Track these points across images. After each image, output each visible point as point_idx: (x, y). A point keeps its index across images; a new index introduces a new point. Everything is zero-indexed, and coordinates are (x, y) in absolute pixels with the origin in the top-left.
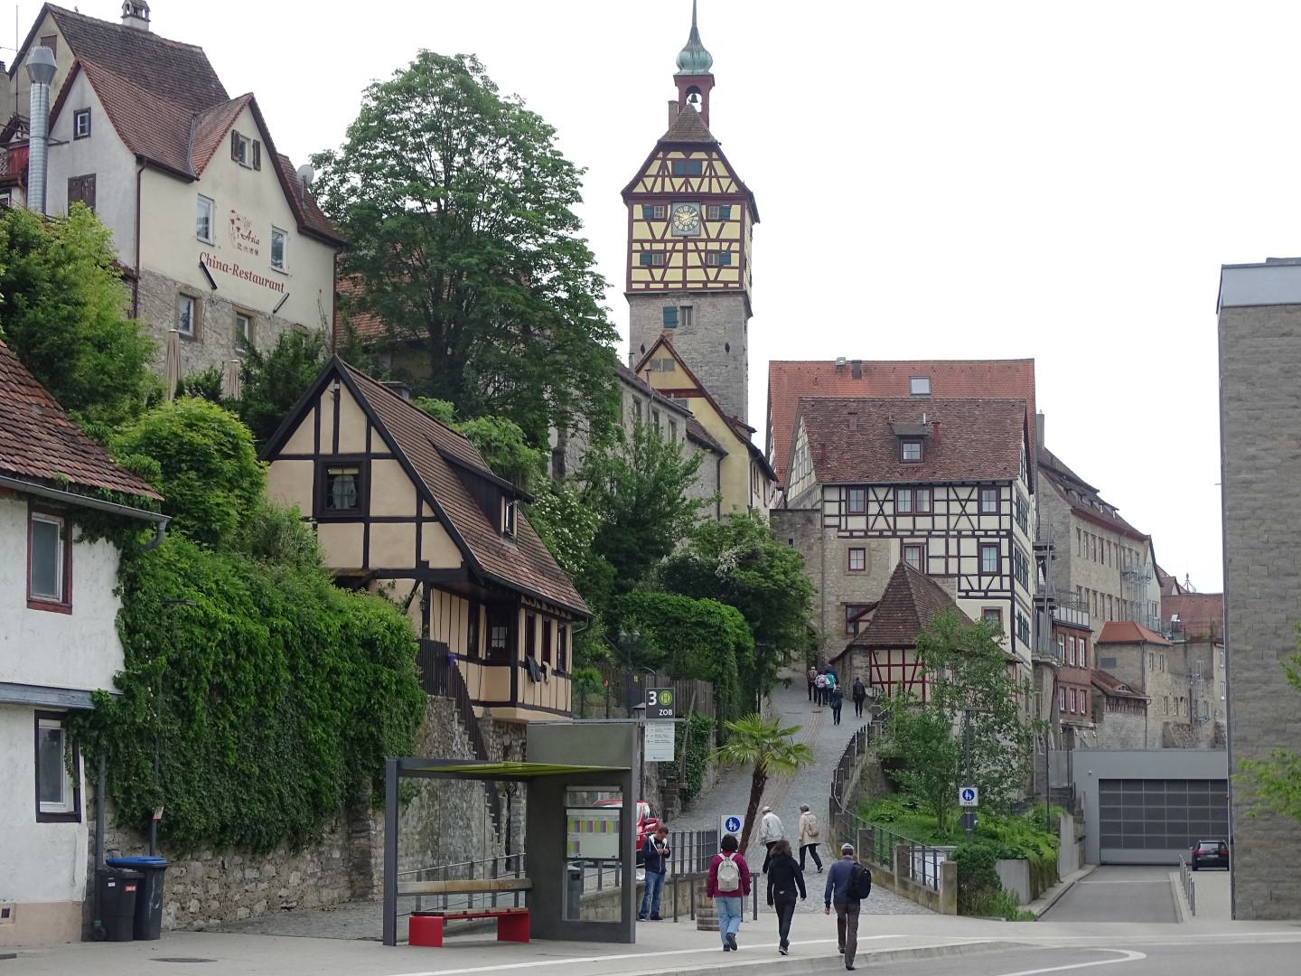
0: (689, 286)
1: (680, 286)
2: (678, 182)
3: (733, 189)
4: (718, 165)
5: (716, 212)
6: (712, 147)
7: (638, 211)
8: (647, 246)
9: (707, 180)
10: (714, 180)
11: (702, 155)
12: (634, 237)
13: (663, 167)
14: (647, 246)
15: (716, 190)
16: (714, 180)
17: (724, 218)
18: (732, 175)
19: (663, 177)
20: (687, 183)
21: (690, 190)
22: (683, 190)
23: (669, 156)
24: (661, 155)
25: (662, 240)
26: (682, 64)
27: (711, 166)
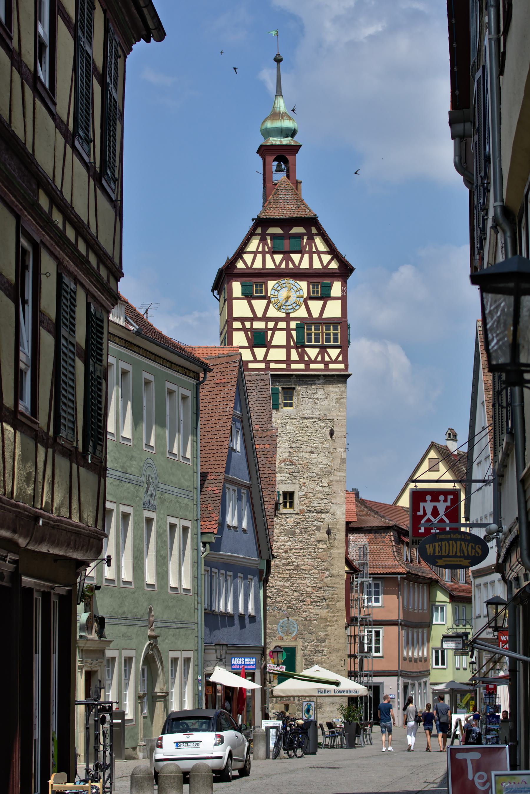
0: (293, 366)
1: (284, 366)
2: (278, 258)
3: (334, 265)
4: (318, 241)
7: (237, 288)
8: (248, 325)
9: (306, 256)
10: (315, 256)
11: (300, 230)
12: (235, 315)
14: (248, 325)
15: (317, 265)
16: (315, 256)
17: (325, 297)
19: (264, 253)
21: (291, 266)
22: (283, 266)
23: (267, 232)
24: (259, 231)
25: (265, 319)
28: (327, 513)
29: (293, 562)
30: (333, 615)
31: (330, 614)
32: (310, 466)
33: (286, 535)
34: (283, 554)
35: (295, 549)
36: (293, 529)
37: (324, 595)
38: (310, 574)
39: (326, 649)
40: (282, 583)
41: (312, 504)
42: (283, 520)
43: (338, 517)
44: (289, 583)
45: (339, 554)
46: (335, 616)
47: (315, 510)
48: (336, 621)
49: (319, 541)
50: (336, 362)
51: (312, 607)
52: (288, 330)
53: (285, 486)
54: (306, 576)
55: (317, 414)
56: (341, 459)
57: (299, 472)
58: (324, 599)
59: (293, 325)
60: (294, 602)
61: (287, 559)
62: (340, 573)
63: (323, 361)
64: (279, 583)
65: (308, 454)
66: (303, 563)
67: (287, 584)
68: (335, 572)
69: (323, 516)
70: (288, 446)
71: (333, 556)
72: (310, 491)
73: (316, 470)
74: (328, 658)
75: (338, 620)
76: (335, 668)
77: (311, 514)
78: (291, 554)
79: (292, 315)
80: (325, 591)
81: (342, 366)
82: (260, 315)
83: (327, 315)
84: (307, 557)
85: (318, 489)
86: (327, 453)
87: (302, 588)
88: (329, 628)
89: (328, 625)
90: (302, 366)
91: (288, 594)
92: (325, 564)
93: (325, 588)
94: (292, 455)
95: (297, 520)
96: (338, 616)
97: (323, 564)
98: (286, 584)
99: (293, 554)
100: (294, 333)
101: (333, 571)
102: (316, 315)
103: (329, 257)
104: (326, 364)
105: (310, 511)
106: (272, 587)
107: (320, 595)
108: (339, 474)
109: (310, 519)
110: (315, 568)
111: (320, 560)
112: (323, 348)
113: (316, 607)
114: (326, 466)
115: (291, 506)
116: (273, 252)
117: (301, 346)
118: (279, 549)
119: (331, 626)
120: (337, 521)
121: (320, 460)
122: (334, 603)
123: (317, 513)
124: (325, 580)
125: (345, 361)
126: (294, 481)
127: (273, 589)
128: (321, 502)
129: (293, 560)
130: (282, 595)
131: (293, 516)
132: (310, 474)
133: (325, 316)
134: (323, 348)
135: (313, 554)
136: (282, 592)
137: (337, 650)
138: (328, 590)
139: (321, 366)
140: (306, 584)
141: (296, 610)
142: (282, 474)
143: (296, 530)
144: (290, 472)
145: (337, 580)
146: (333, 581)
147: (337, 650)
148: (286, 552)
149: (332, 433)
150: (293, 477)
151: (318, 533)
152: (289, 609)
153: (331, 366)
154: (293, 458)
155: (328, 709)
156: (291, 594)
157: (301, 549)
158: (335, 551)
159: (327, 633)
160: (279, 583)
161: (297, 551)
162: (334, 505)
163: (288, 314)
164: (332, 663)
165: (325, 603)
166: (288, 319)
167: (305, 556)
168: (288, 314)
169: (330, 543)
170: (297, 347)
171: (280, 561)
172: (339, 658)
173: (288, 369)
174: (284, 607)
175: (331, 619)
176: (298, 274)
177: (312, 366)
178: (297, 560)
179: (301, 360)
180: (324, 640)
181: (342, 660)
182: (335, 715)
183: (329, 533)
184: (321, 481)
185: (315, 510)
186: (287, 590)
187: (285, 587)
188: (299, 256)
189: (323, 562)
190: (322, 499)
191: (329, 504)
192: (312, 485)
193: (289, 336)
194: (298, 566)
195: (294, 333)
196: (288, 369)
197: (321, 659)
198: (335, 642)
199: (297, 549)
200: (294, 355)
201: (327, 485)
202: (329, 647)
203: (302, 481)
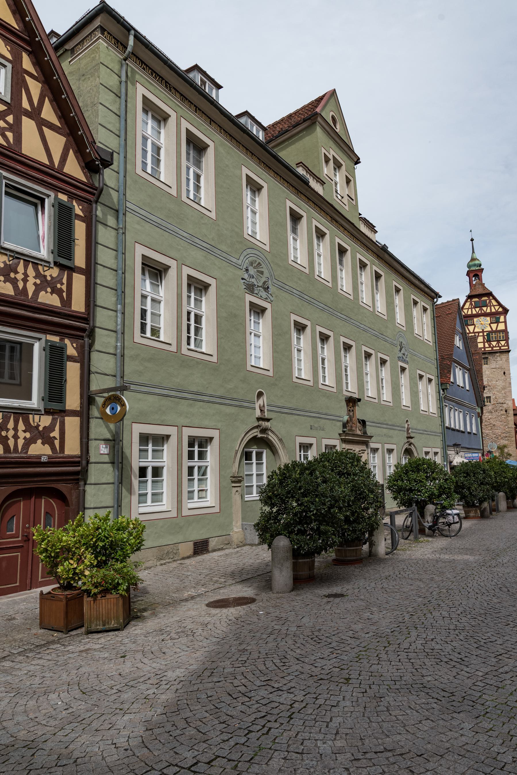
0: (487, 349)
2: (477, 309)
5: (494, 320)
6: (490, 294)
9: (489, 308)
10: (492, 307)
11: (486, 298)
13: (471, 304)
15: (493, 310)
16: (492, 307)
17: (498, 322)
18: (500, 304)
19: (471, 308)
20: (481, 309)
22: (480, 312)
24: (469, 300)
26: (469, 266)
27: (490, 302)
50: (504, 346)
52: (483, 336)
55: (498, 366)
59: (485, 334)
63: (499, 346)
67: (491, 432)
73: (499, 388)
79: (485, 330)
81: (507, 348)
82: (472, 331)
83: (498, 329)
90: (490, 349)
100: (486, 337)
102: (494, 329)
103: (498, 307)
104: (500, 347)
112: (498, 341)
115: (490, 402)
116: (475, 307)
117: (489, 341)
125: (508, 345)
133: (498, 329)
134: (498, 341)
139: (498, 348)
140: (498, 432)
145: (511, 429)
149: (504, 373)
153: (502, 348)
158: (509, 418)
163: (483, 330)
166: (483, 332)
168: (483, 330)
170: (487, 342)
173: (485, 350)
176: (486, 315)
177: (494, 349)
179: (490, 347)
183: (506, 411)
188: (486, 308)
193: (484, 338)
195: (486, 337)
196: (485, 350)
200: (487, 345)
203: (494, 392)
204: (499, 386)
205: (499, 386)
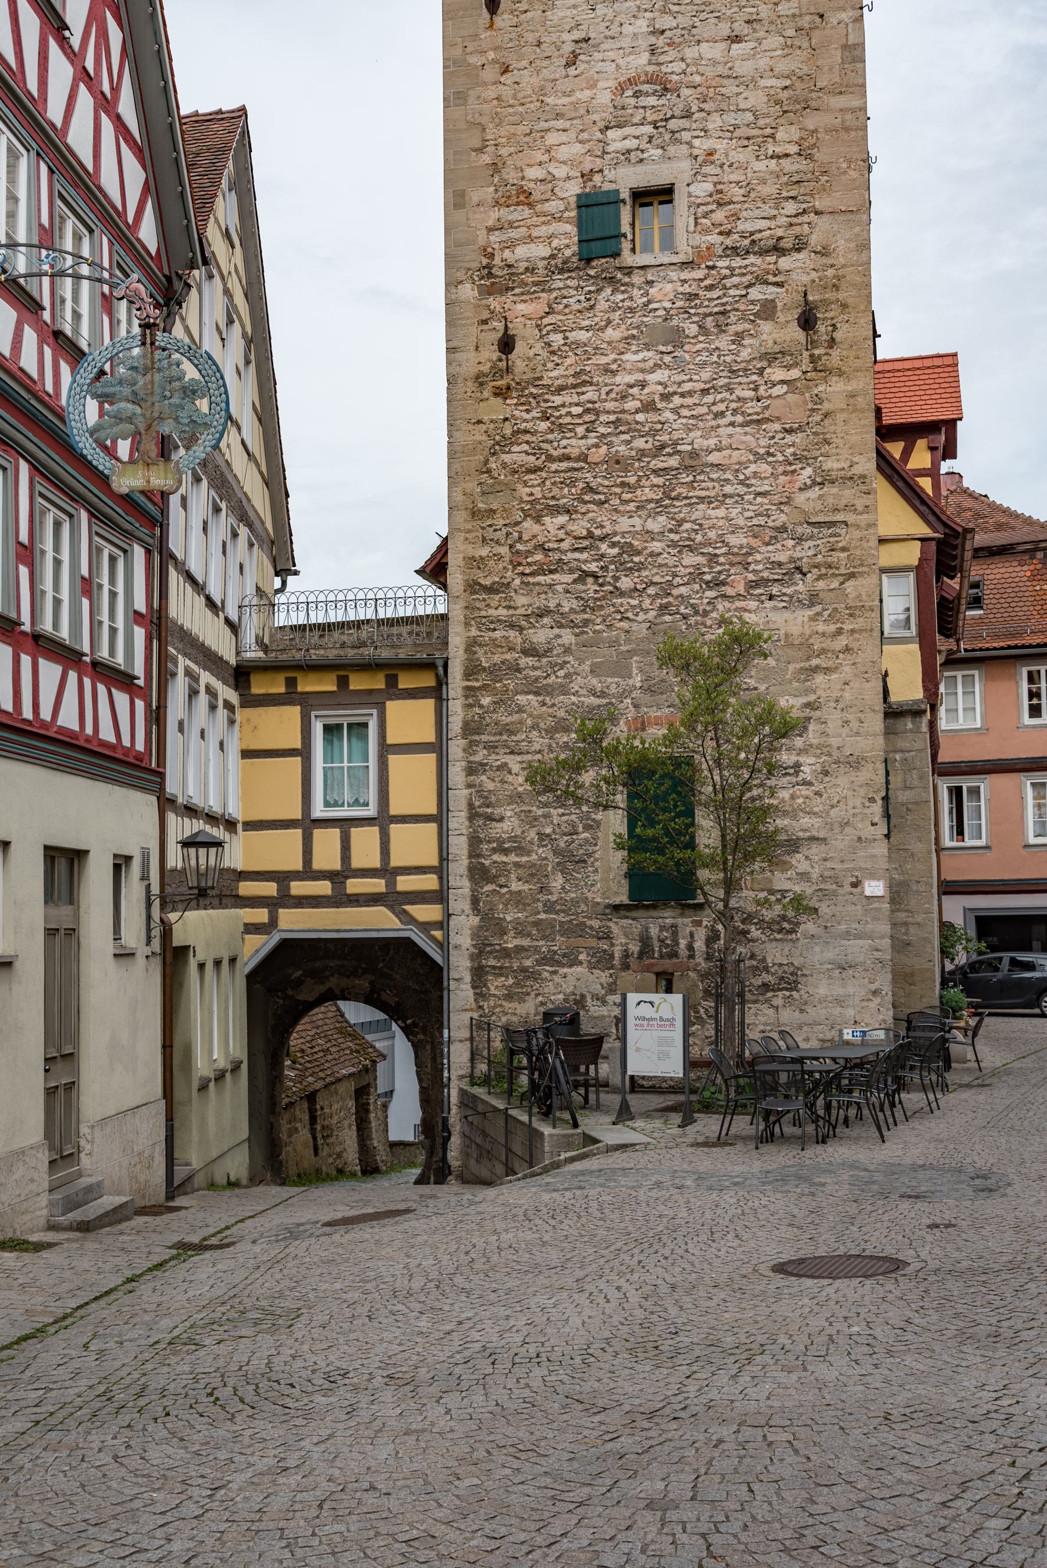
28: (799, 250)
29: (676, 443)
30: (832, 628)
31: (821, 627)
32: (730, 89)
33: (647, 347)
34: (640, 417)
35: (682, 395)
36: (675, 322)
37: (799, 555)
38: (741, 483)
39: (811, 760)
40: (637, 521)
41: (742, 226)
42: (636, 292)
43: (842, 260)
44: (662, 519)
45: (852, 396)
46: (839, 632)
47: (753, 242)
48: (847, 649)
49: (770, 358)
51: (753, 604)
53: (640, 168)
54: (728, 489)
56: (845, 47)
57: (687, 115)
58: (799, 569)
60: (683, 590)
61: (653, 433)
62: (857, 470)
64: (624, 523)
65: (723, 45)
66: (712, 442)
68: (836, 465)
69: (785, 263)
70: (645, 29)
71: (826, 406)
72: (734, 177)
73: (755, 99)
74: (818, 794)
75: (855, 645)
76: (848, 830)
77: (737, 262)
78: (668, 415)
80: (800, 539)
84: (729, 418)
85: (760, 166)
86: (791, 32)
87: (712, 534)
88: (820, 679)
89: (816, 669)
91: (660, 560)
92: (798, 438)
93: (799, 530)
94: (662, 59)
95: (686, 288)
96: (853, 631)
97: (789, 439)
98: (653, 525)
99: (675, 411)
101: (830, 464)
105: (734, 251)
106: (602, 539)
107: (782, 557)
108: (838, 102)
109: (736, 280)
110: (758, 457)
111: (777, 426)
113: (769, 604)
114: (788, 83)
115: (668, 244)
118: (624, 397)
119: (827, 670)
120: (834, 277)
121: (763, 63)
122: (835, 584)
123: (763, 252)
124: (800, 499)
126: (672, 150)
127: (604, 547)
128: (775, 212)
129: (676, 435)
130: (640, 567)
131: (673, 275)
132: (730, 119)
135: (752, 407)
136: (639, 553)
137: (855, 763)
138: (811, 537)
140: (726, 521)
141: (692, 620)
142: (628, 130)
143: (686, 325)
144: (655, 117)
146: (831, 501)
147: (855, 763)
148: (648, 407)
150: (667, 137)
151: (766, 326)
152: (668, 618)
154: (664, 68)
155: (822, 991)
156: (671, 562)
157: (705, 392)
158: (835, 389)
159: (812, 698)
160: (624, 523)
161: (689, 401)
162: (825, 218)
164: (834, 812)
165: (801, 587)
167: (721, 414)
169: (813, 360)
171: (628, 442)
172: (862, 792)
174: (646, 611)
175: (828, 643)
178: (692, 435)
180: (799, 727)
181: (872, 800)
182: (851, 1012)
183: (807, 321)
184: (772, 136)
185: (753, 242)
186: (656, 546)
187: (650, 535)
189: (789, 431)
190: (779, 201)
191: (805, 218)
192: (739, 156)
194: (694, 454)
197: (793, 797)
198: (845, 731)
199: (690, 393)
201: (793, 149)
202: (823, 749)
203: (702, 145)
204: (750, 83)
205: (750, 83)
